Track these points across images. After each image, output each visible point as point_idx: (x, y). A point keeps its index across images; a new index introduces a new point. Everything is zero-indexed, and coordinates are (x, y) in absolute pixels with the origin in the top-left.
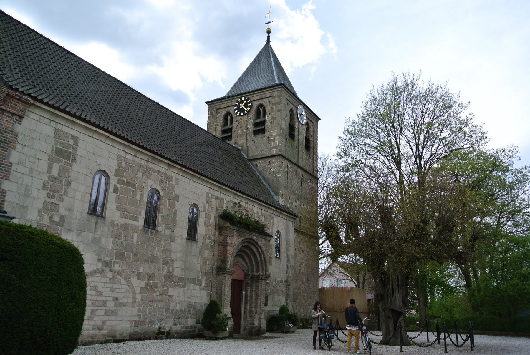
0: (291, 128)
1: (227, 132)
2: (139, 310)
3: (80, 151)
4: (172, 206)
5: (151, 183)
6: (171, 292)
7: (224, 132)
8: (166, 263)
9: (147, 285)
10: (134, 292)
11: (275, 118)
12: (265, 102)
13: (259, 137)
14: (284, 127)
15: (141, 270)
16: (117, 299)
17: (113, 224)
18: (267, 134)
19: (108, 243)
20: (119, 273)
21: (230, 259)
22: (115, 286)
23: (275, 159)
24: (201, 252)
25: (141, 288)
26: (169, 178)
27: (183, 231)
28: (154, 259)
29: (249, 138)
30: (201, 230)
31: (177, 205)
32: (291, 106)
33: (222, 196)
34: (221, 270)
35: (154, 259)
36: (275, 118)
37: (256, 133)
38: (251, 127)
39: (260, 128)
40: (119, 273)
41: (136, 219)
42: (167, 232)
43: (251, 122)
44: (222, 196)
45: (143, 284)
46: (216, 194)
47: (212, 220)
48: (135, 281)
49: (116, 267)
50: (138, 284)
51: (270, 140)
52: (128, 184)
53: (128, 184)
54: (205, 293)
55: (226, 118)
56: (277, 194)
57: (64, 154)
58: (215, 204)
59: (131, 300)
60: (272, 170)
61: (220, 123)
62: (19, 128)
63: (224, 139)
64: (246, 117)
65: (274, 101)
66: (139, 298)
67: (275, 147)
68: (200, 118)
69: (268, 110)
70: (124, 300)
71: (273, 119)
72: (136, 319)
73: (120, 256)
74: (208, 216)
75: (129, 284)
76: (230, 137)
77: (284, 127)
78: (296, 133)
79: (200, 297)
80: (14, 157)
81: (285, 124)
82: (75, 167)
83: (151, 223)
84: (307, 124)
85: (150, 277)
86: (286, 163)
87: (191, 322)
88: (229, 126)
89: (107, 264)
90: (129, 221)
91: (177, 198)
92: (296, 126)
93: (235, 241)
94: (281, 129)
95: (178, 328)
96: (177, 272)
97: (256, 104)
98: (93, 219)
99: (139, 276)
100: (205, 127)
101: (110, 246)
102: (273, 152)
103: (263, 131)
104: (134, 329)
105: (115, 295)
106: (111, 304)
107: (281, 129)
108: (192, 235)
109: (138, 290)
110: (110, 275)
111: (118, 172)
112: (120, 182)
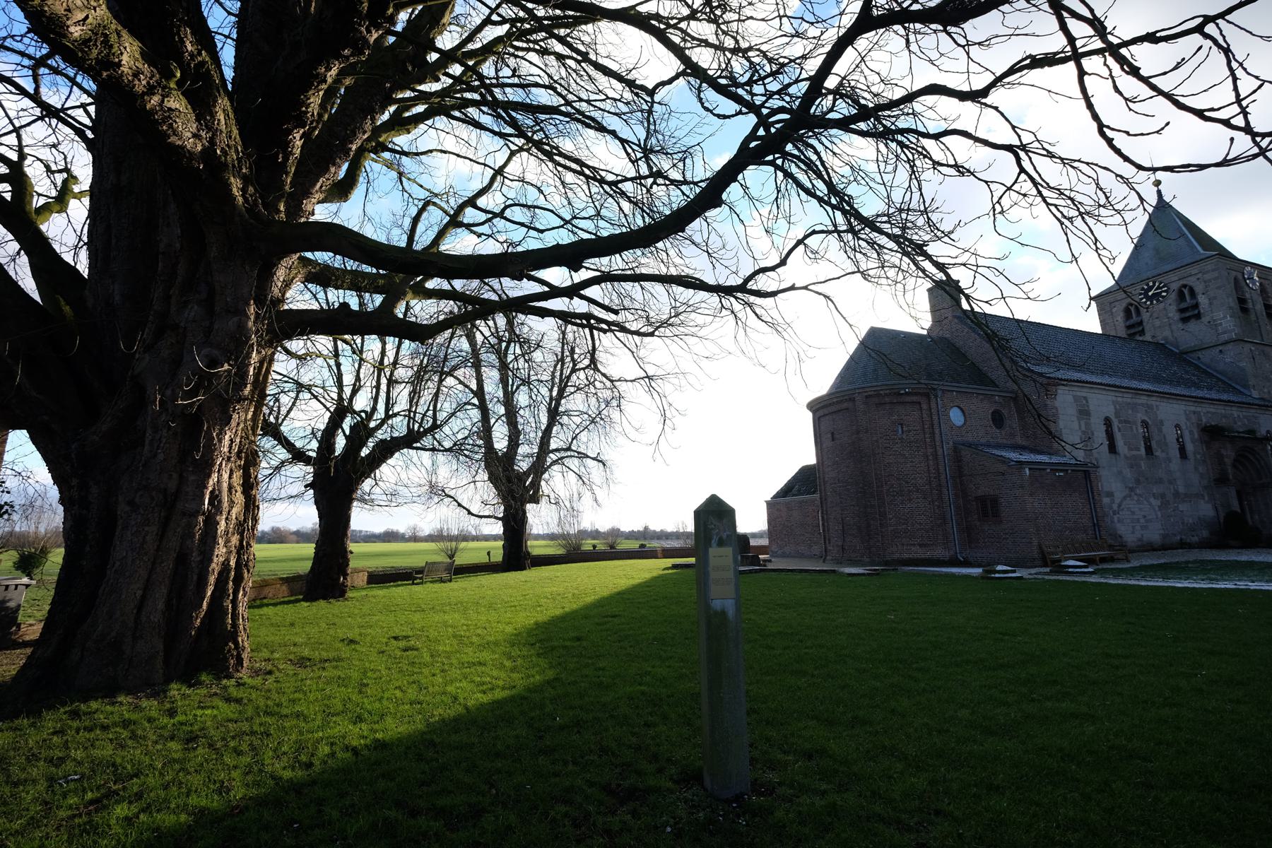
0: (1242, 301)
1: (1135, 328)
3: (1091, 408)
4: (1160, 430)
5: (1141, 416)
6: (1181, 507)
7: (1128, 327)
8: (1170, 483)
11: (1215, 298)
12: (1191, 281)
13: (1193, 326)
14: (1232, 304)
17: (1126, 457)
18: (1205, 319)
19: (1128, 473)
21: (1230, 470)
23: (1230, 346)
24: (1196, 468)
26: (1150, 407)
27: (1175, 453)
28: (1160, 481)
29: (1174, 327)
30: (1190, 447)
31: (1164, 429)
32: (1234, 273)
33: (1199, 409)
34: (1221, 480)
35: (1160, 481)
36: (1215, 298)
37: (1185, 320)
38: (1177, 316)
39: (1190, 313)
41: (1138, 450)
42: (1163, 455)
43: (1173, 308)
44: (1199, 409)
45: (1159, 503)
46: (1193, 408)
47: (1196, 436)
48: (1152, 500)
51: (1213, 325)
52: (1126, 422)
53: (1126, 422)
54: (1209, 506)
55: (1127, 312)
56: (1246, 386)
57: (1084, 413)
58: (1194, 418)
60: (1228, 360)
61: (1120, 317)
62: (1057, 404)
63: (1131, 336)
64: (1162, 305)
65: (1207, 277)
67: (1224, 333)
68: (1091, 323)
69: (1199, 288)
71: (1211, 301)
73: (1138, 481)
74: (1191, 432)
75: (1150, 504)
76: (1142, 333)
77: (1232, 304)
78: (1250, 305)
79: (1206, 509)
80: (1061, 424)
81: (1232, 302)
82: (1092, 421)
83: (1149, 450)
84: (1261, 284)
85: (1163, 496)
86: (1248, 346)
87: (1205, 533)
88: (1135, 319)
89: (1131, 489)
90: (1135, 453)
91: (1162, 422)
92: (1248, 296)
93: (1229, 453)
94: (1231, 308)
95: (1196, 539)
96: (1181, 490)
97: (1175, 286)
98: (1113, 456)
100: (1100, 331)
101: (1129, 475)
102: (1226, 337)
103: (1198, 316)
106: (1142, 521)
107: (1231, 308)
108: (1183, 453)
111: (1117, 414)
112: (1120, 422)
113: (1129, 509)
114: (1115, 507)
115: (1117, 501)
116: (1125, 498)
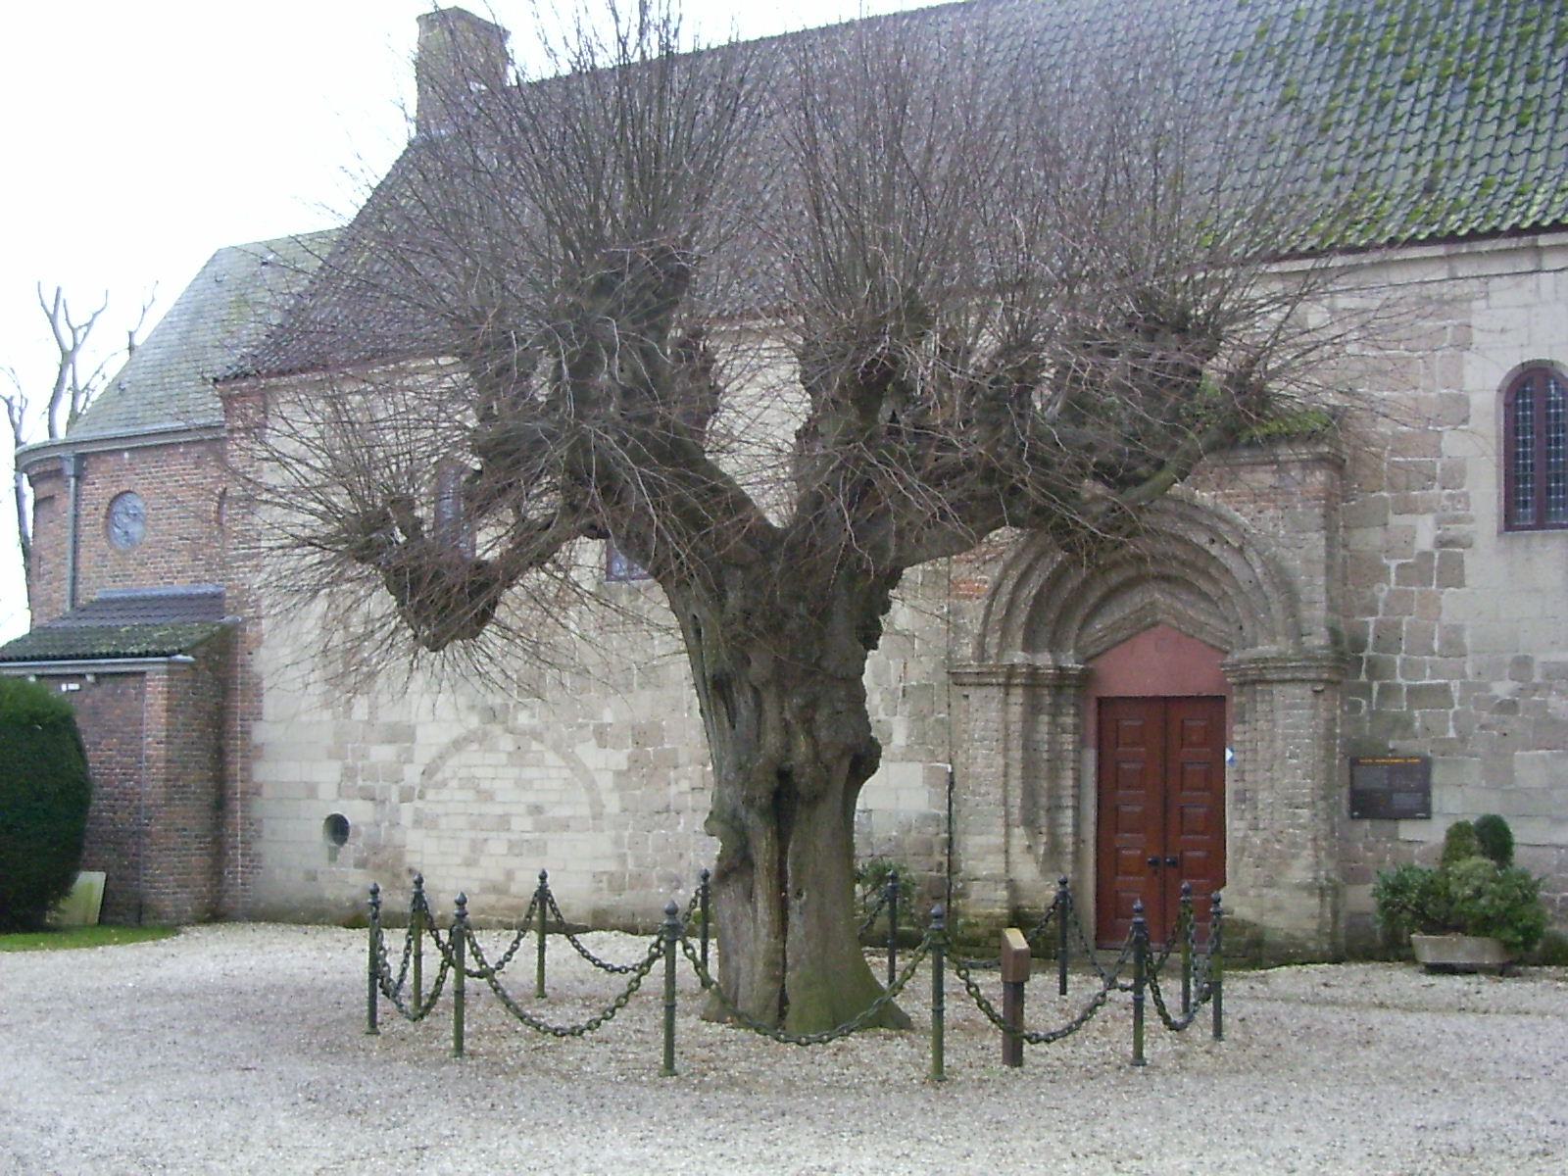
2: (617, 842)
9: (634, 761)
10: (591, 786)
15: (608, 717)
16: (536, 810)
20: (536, 735)
22: (530, 773)
25: (619, 774)
40: (536, 735)
45: (620, 758)
48: (589, 753)
49: (523, 719)
50: (604, 762)
59: (585, 811)
66: (613, 804)
70: (564, 812)
72: (612, 866)
85: (642, 735)
99: (601, 735)
104: (607, 900)
105: (531, 798)
106: (522, 824)
109: (606, 781)
110: (507, 743)
113: (470, 783)
114: (412, 775)
115: (423, 755)
116: (458, 745)
